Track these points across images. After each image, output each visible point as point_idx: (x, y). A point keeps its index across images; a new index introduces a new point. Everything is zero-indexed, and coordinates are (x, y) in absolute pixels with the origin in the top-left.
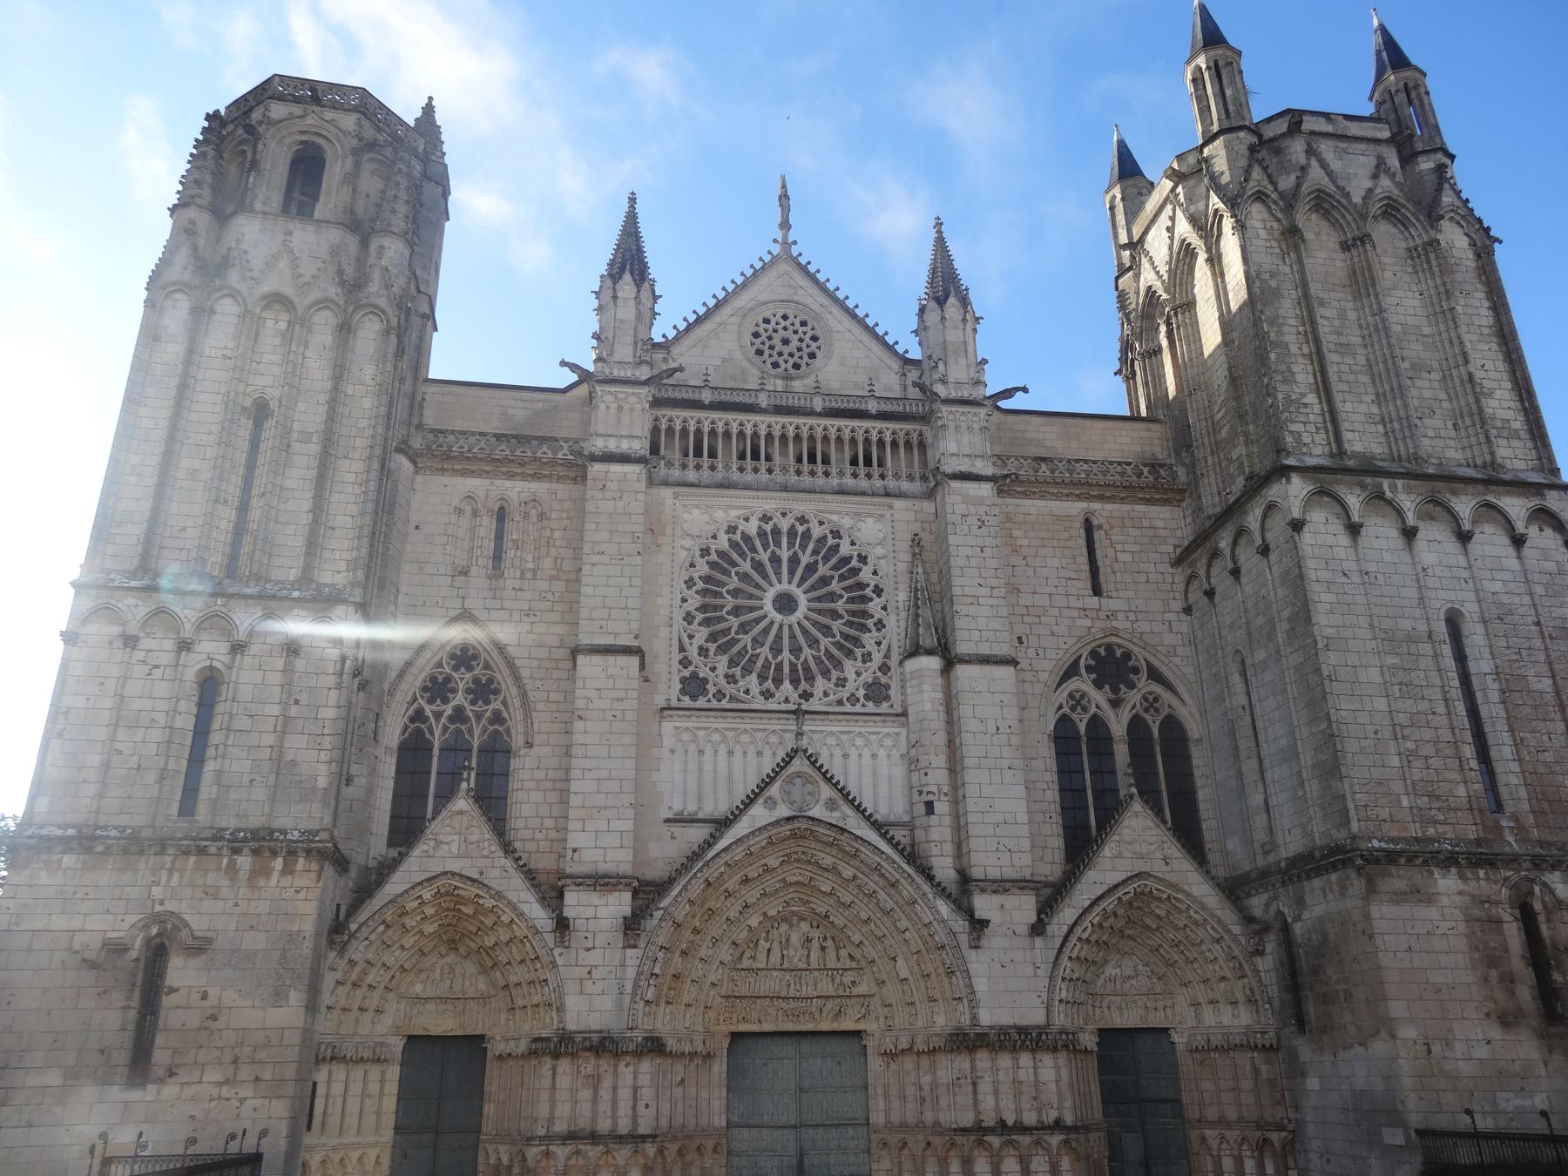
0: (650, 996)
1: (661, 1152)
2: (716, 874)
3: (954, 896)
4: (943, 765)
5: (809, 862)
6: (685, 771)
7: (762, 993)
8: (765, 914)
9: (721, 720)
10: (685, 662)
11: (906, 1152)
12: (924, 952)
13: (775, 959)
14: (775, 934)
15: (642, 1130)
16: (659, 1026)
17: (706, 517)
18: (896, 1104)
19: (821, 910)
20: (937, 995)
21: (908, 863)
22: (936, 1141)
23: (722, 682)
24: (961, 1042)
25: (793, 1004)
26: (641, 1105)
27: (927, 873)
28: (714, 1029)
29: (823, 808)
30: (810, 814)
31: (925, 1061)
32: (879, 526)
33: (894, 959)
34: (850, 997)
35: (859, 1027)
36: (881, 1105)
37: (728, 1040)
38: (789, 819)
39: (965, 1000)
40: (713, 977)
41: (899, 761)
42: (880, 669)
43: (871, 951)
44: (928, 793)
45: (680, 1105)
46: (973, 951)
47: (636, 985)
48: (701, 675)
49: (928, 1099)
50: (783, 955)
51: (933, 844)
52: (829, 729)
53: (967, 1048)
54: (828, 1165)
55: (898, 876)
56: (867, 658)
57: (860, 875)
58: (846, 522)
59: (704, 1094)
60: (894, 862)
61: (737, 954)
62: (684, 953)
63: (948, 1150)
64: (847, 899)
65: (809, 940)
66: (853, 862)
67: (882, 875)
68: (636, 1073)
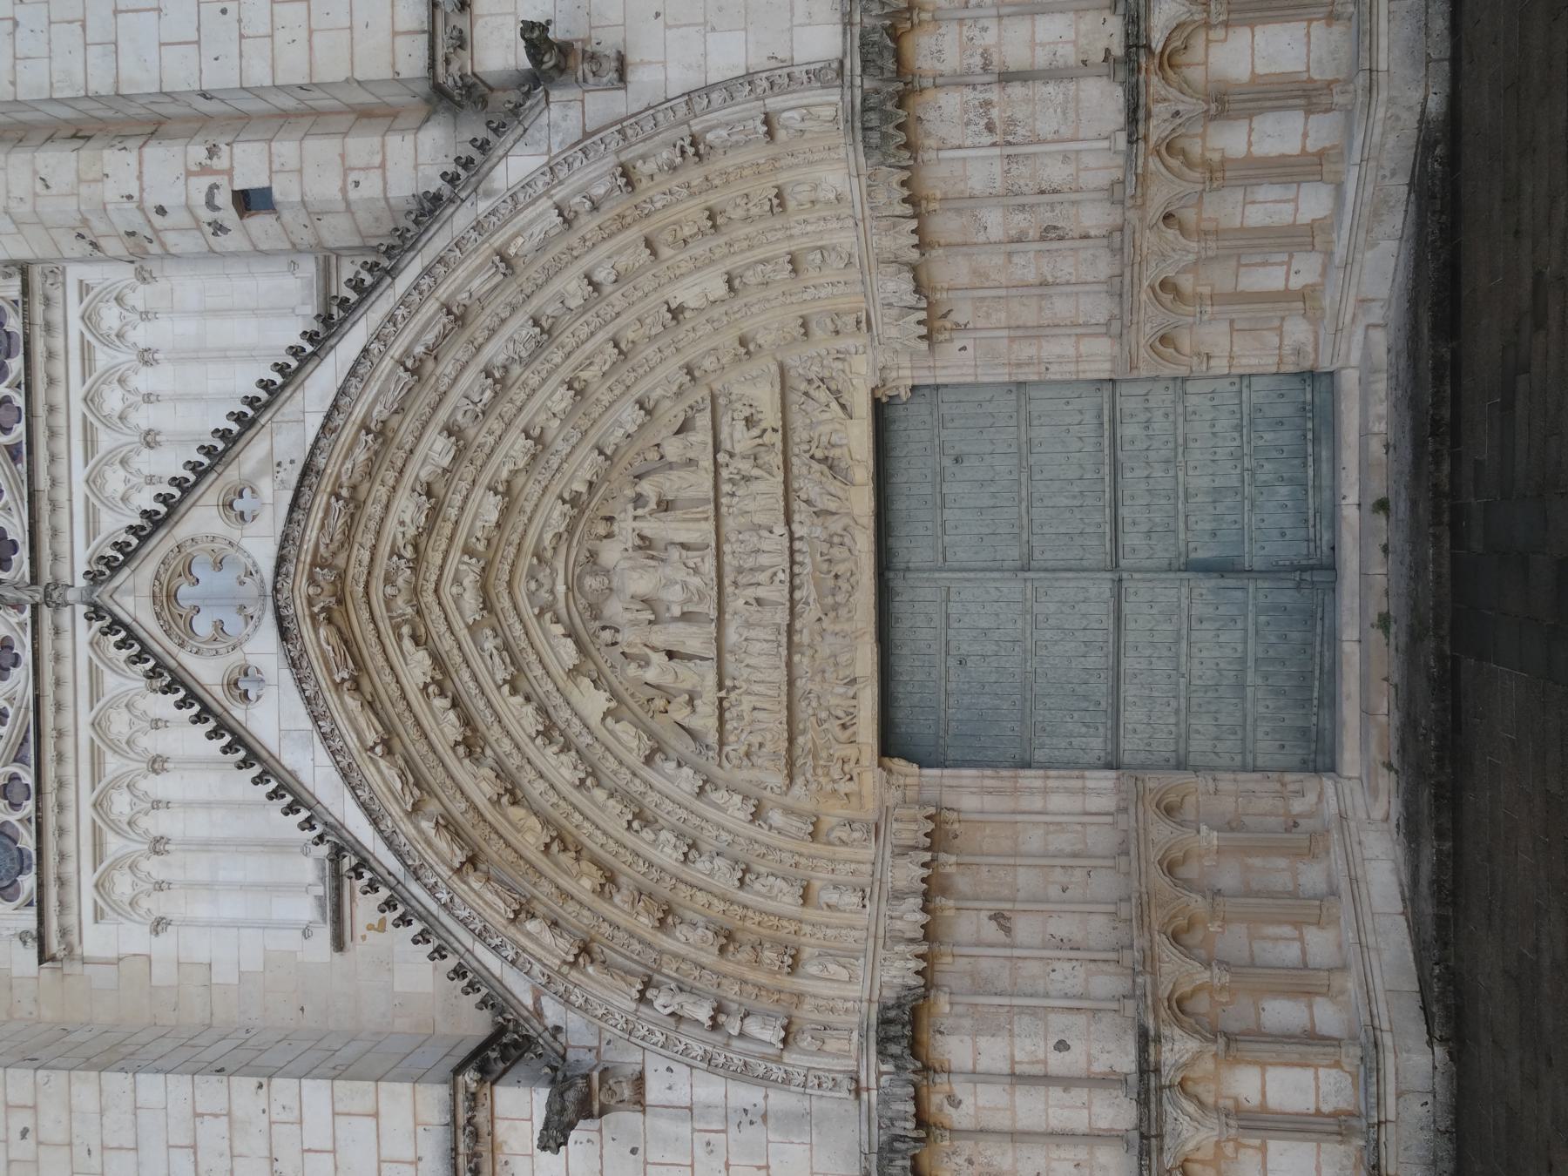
0: (773, 1035)
1: (1180, 1006)
2: (442, 843)
3: (482, 133)
4: (131, 157)
5: (416, 564)
6: (209, 886)
7: (781, 676)
8: (574, 672)
9: (69, 795)
11: (1186, 283)
12: (646, 228)
13: (694, 639)
14: (630, 638)
15: (1126, 1062)
16: (855, 991)
18: (1062, 307)
19: (556, 516)
20: (763, 190)
21: (392, 273)
22: (1160, 196)
24: (886, 118)
25: (806, 592)
26: (1058, 1063)
27: (430, 207)
28: (870, 812)
29: (251, 528)
30: (267, 567)
31: (945, 225)
33: (676, 313)
34: (786, 431)
36: (1065, 347)
37: (898, 764)
38: (284, 634)
39: (773, 103)
40: (735, 812)
41: (162, 285)
43: (661, 379)
44: (211, 204)
45: (1063, 927)
46: (635, 76)
47: (744, 1074)
49: (1048, 217)
50: (686, 617)
51: (353, 195)
52: (80, 489)
53: (901, 100)
54: (1217, 493)
55: (431, 307)
57: (443, 415)
59: (1033, 840)
60: (391, 318)
61: (684, 745)
62: (666, 917)
63: (1189, 164)
64: (517, 447)
65: (645, 544)
66: (405, 436)
67: (434, 352)
68: (976, 1076)
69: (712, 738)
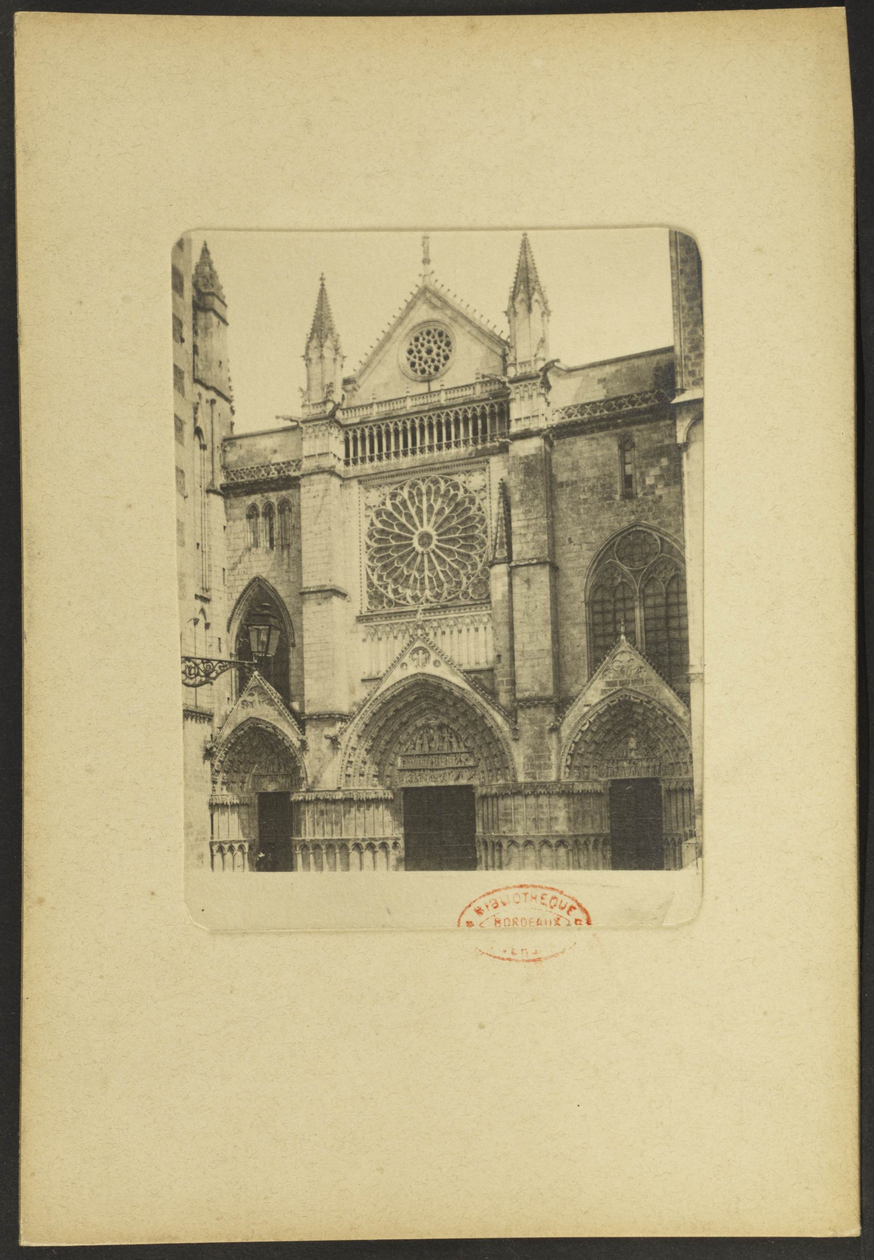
10: (371, 585)
17: (378, 493)
23: (391, 596)
32: (482, 477)
35: (470, 783)
42: (482, 573)
48: (379, 593)
50: (430, 747)
56: (474, 566)
58: (459, 479)
69: (406, 754)
